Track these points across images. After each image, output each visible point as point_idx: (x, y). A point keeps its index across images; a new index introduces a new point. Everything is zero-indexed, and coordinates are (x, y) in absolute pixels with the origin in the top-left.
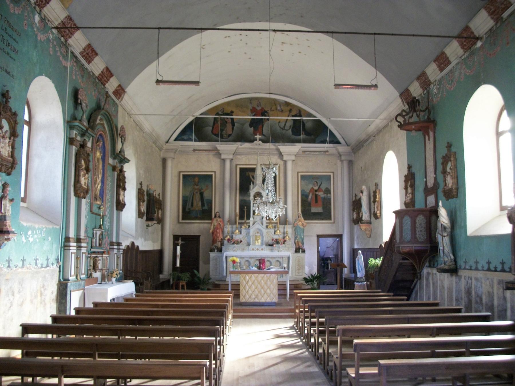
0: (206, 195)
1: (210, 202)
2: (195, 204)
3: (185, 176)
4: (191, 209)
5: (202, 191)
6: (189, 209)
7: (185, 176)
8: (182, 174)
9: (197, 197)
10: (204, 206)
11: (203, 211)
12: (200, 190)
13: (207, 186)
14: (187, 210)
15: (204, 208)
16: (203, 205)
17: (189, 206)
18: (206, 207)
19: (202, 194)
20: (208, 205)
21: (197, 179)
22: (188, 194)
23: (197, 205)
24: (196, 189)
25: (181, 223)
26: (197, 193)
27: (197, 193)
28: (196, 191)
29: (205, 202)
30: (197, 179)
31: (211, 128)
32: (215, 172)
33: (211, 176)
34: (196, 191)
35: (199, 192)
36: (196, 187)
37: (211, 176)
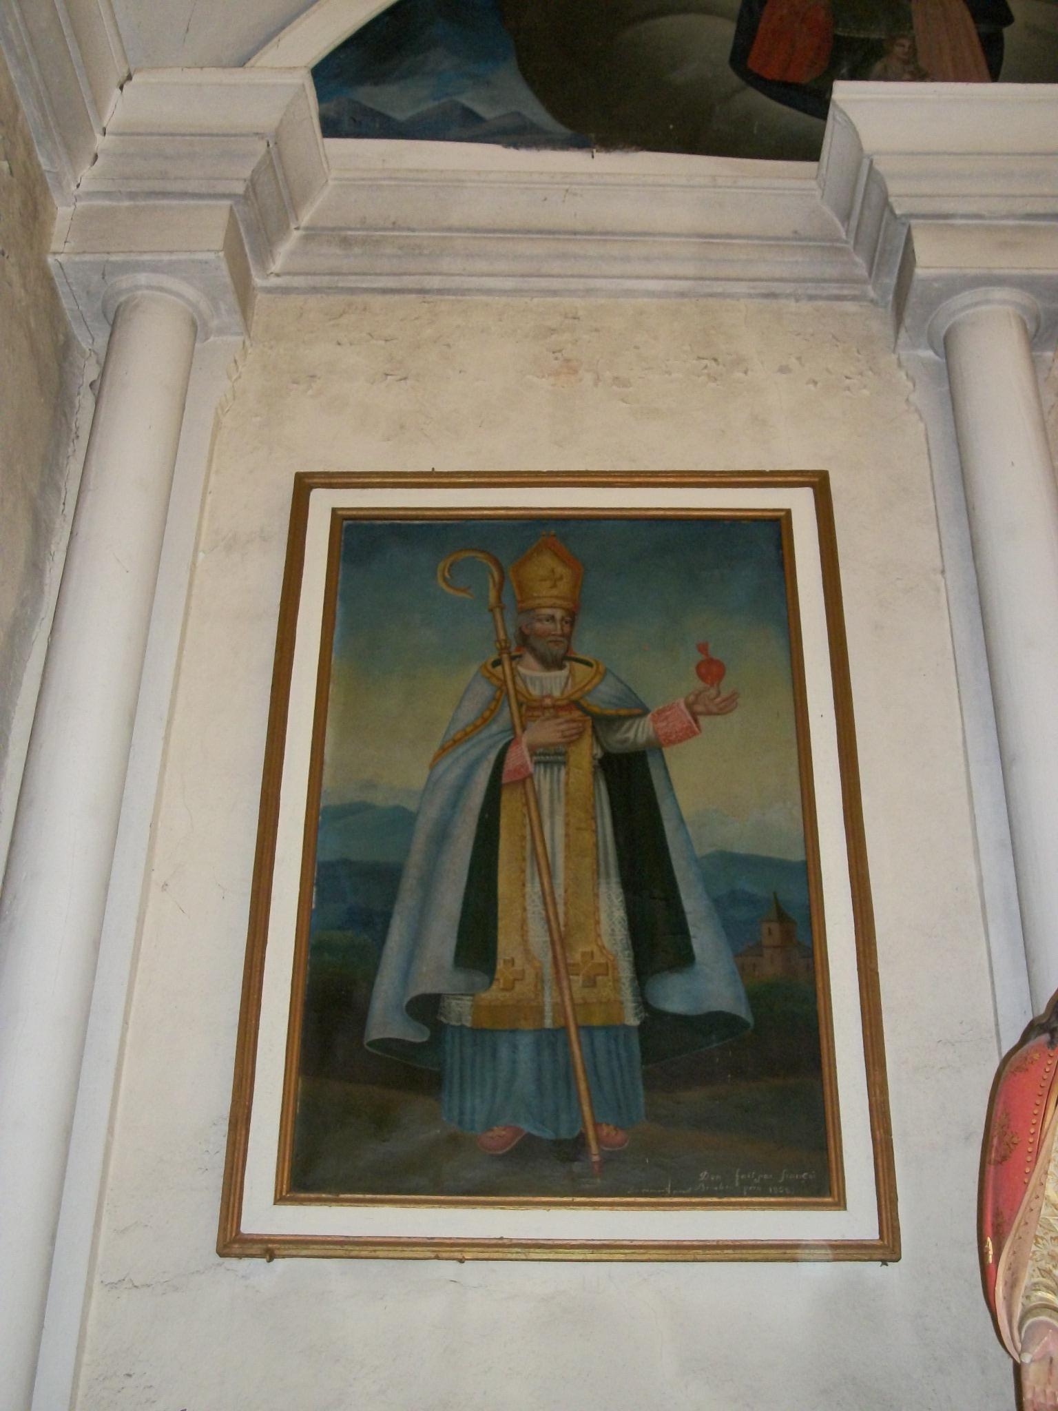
0: (706, 794)
1: (778, 914)
2: (522, 934)
3: (358, 538)
4: (460, 1011)
5: (639, 732)
6: (426, 1008)
7: (358, 538)
8: (322, 503)
9: (563, 820)
10: (684, 958)
11: (669, 1048)
12: (602, 723)
13: (711, 670)
14: (386, 1019)
15: (675, 996)
16: (657, 938)
17: (417, 955)
18: (711, 982)
19: (630, 785)
20: (745, 954)
21: (548, 581)
22: (406, 771)
23: (560, 941)
24: (531, 709)
25: (270, 1248)
26: (552, 757)
27: (552, 757)
28: (545, 732)
29: (694, 903)
30: (548, 581)
31: (727, 30)
32: (819, 484)
33: (777, 526)
34: (545, 732)
35: (585, 754)
36: (547, 683)
37: (777, 526)
